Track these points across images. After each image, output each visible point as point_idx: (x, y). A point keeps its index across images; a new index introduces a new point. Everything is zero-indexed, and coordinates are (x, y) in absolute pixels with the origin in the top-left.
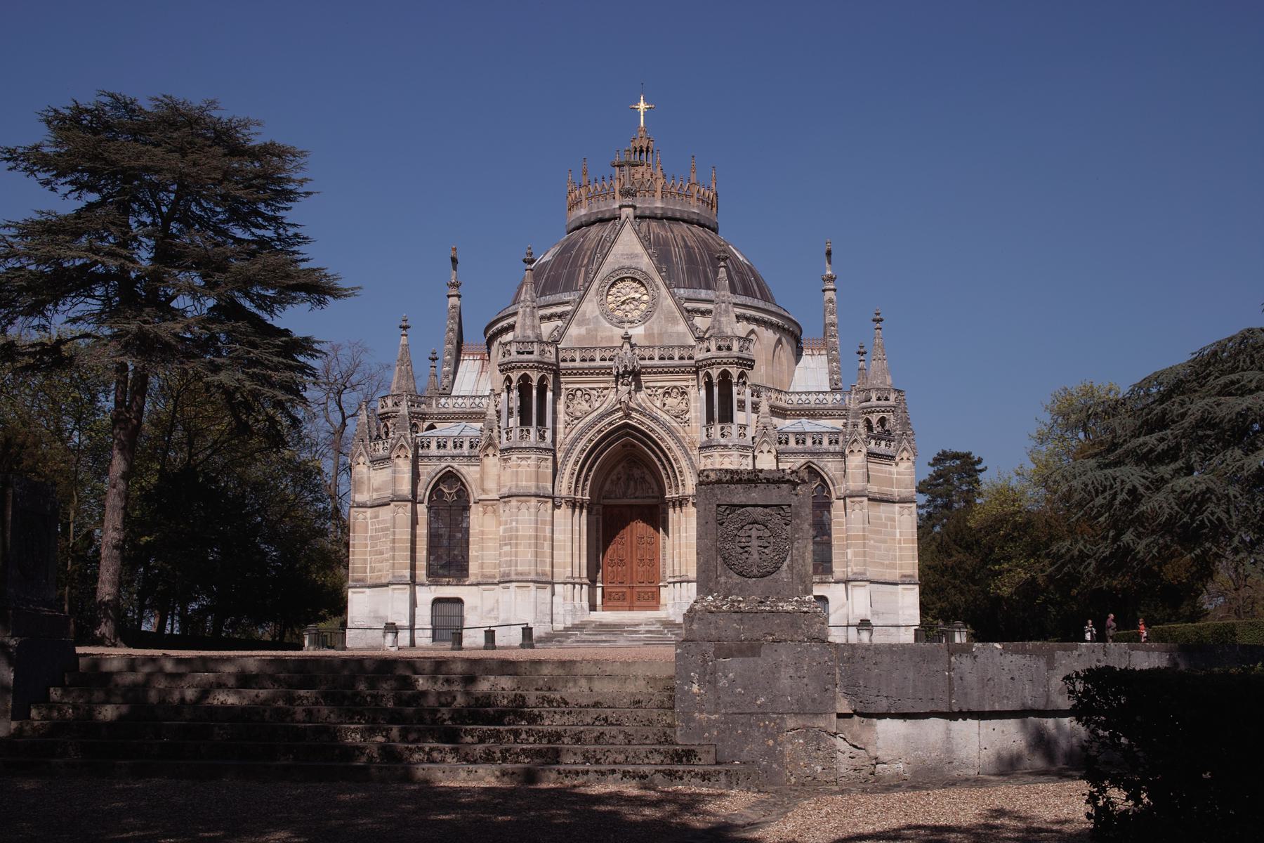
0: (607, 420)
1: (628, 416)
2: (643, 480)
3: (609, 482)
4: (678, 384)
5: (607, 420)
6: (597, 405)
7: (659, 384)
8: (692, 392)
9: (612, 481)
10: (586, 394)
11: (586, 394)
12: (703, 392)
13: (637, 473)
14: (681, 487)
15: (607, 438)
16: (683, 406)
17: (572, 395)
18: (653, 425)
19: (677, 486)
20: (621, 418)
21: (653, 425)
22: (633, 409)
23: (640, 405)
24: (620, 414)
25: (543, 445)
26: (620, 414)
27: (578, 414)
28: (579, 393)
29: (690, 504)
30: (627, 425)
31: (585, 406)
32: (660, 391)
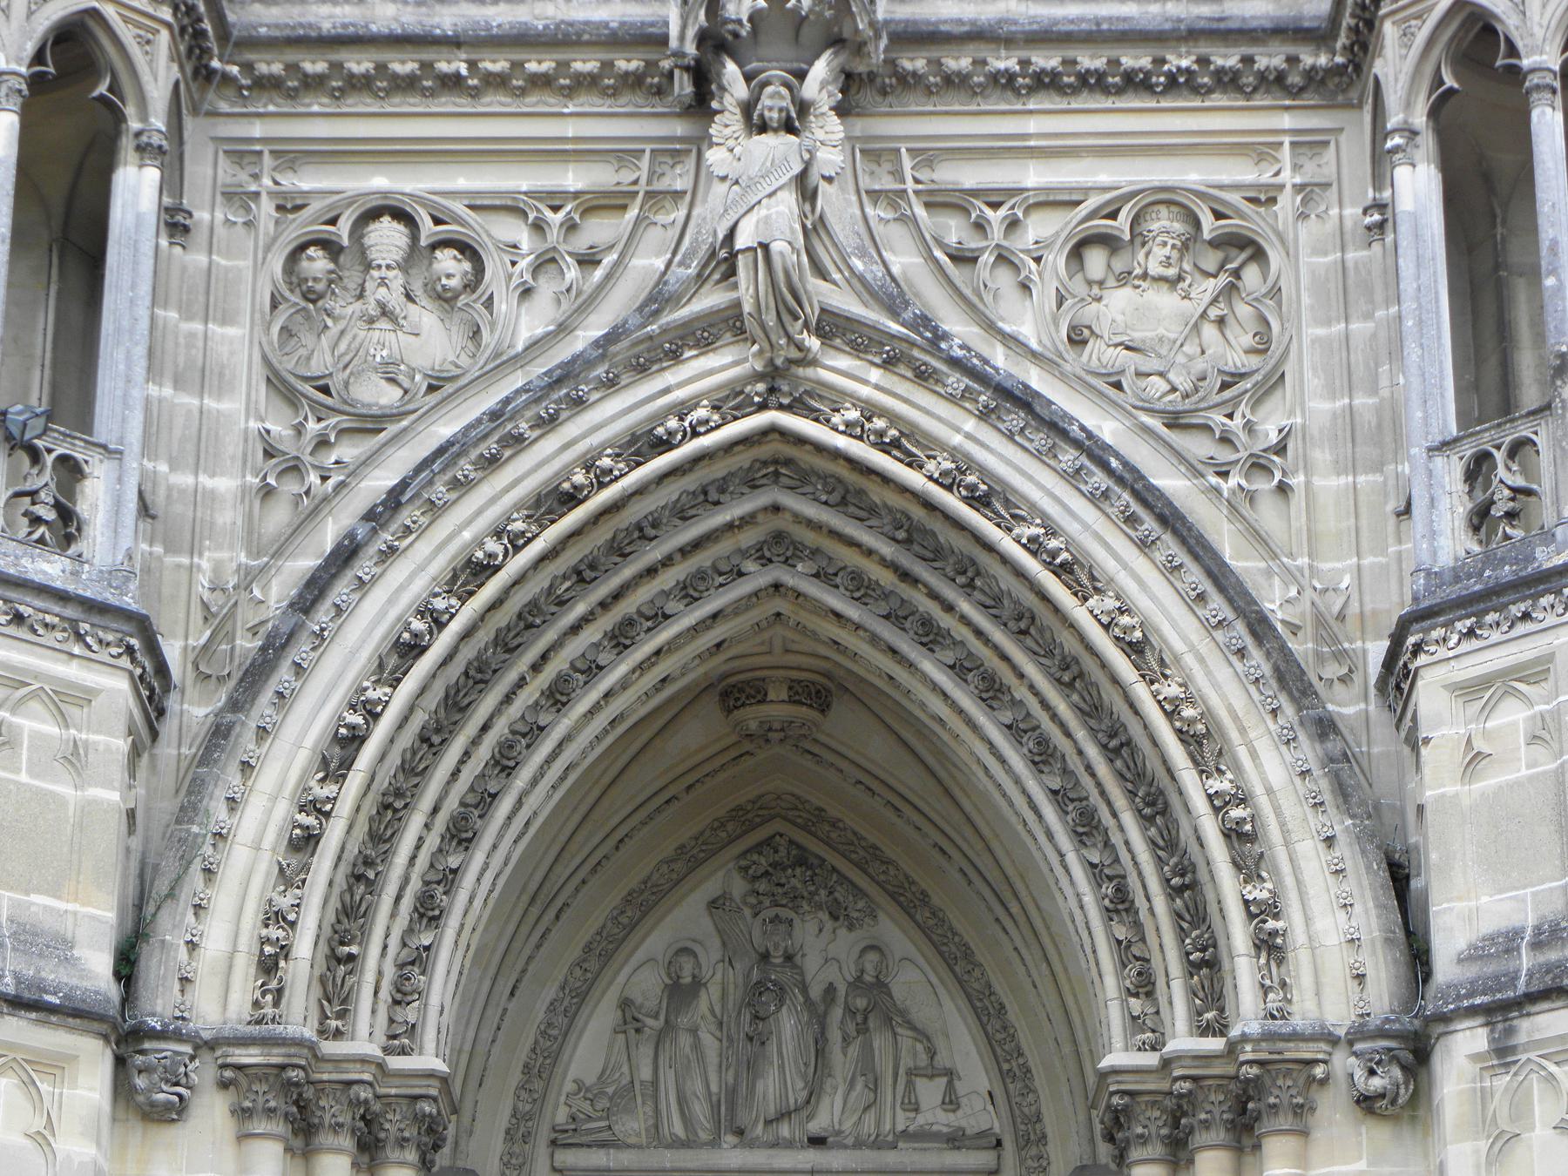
0: (612, 414)
1: (778, 381)
2: (874, 1004)
3: (600, 1019)
4: (1191, 174)
5: (612, 414)
6: (530, 323)
7: (1033, 176)
8: (1305, 250)
9: (630, 1017)
10: (447, 250)
11: (447, 250)
12: (1418, 187)
13: (825, 951)
14: (1244, 969)
15: (601, 551)
16: (1232, 349)
17: (322, 260)
18: (1002, 456)
19: (1207, 965)
20: (731, 402)
21: (1002, 456)
22: (832, 327)
23: (892, 299)
24: (721, 365)
25: (50, 568)
26: (721, 365)
27: (378, 394)
28: (387, 238)
29: (1333, 1111)
30: (777, 459)
31: (430, 340)
32: (1039, 227)
